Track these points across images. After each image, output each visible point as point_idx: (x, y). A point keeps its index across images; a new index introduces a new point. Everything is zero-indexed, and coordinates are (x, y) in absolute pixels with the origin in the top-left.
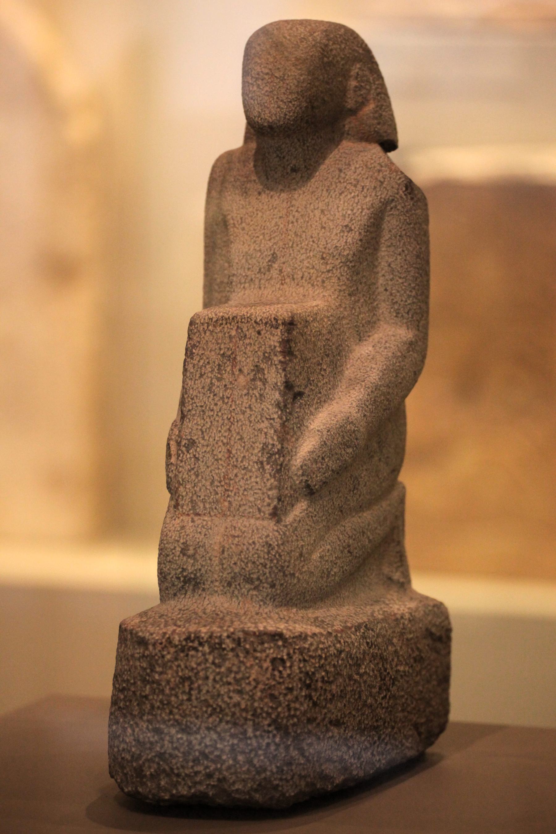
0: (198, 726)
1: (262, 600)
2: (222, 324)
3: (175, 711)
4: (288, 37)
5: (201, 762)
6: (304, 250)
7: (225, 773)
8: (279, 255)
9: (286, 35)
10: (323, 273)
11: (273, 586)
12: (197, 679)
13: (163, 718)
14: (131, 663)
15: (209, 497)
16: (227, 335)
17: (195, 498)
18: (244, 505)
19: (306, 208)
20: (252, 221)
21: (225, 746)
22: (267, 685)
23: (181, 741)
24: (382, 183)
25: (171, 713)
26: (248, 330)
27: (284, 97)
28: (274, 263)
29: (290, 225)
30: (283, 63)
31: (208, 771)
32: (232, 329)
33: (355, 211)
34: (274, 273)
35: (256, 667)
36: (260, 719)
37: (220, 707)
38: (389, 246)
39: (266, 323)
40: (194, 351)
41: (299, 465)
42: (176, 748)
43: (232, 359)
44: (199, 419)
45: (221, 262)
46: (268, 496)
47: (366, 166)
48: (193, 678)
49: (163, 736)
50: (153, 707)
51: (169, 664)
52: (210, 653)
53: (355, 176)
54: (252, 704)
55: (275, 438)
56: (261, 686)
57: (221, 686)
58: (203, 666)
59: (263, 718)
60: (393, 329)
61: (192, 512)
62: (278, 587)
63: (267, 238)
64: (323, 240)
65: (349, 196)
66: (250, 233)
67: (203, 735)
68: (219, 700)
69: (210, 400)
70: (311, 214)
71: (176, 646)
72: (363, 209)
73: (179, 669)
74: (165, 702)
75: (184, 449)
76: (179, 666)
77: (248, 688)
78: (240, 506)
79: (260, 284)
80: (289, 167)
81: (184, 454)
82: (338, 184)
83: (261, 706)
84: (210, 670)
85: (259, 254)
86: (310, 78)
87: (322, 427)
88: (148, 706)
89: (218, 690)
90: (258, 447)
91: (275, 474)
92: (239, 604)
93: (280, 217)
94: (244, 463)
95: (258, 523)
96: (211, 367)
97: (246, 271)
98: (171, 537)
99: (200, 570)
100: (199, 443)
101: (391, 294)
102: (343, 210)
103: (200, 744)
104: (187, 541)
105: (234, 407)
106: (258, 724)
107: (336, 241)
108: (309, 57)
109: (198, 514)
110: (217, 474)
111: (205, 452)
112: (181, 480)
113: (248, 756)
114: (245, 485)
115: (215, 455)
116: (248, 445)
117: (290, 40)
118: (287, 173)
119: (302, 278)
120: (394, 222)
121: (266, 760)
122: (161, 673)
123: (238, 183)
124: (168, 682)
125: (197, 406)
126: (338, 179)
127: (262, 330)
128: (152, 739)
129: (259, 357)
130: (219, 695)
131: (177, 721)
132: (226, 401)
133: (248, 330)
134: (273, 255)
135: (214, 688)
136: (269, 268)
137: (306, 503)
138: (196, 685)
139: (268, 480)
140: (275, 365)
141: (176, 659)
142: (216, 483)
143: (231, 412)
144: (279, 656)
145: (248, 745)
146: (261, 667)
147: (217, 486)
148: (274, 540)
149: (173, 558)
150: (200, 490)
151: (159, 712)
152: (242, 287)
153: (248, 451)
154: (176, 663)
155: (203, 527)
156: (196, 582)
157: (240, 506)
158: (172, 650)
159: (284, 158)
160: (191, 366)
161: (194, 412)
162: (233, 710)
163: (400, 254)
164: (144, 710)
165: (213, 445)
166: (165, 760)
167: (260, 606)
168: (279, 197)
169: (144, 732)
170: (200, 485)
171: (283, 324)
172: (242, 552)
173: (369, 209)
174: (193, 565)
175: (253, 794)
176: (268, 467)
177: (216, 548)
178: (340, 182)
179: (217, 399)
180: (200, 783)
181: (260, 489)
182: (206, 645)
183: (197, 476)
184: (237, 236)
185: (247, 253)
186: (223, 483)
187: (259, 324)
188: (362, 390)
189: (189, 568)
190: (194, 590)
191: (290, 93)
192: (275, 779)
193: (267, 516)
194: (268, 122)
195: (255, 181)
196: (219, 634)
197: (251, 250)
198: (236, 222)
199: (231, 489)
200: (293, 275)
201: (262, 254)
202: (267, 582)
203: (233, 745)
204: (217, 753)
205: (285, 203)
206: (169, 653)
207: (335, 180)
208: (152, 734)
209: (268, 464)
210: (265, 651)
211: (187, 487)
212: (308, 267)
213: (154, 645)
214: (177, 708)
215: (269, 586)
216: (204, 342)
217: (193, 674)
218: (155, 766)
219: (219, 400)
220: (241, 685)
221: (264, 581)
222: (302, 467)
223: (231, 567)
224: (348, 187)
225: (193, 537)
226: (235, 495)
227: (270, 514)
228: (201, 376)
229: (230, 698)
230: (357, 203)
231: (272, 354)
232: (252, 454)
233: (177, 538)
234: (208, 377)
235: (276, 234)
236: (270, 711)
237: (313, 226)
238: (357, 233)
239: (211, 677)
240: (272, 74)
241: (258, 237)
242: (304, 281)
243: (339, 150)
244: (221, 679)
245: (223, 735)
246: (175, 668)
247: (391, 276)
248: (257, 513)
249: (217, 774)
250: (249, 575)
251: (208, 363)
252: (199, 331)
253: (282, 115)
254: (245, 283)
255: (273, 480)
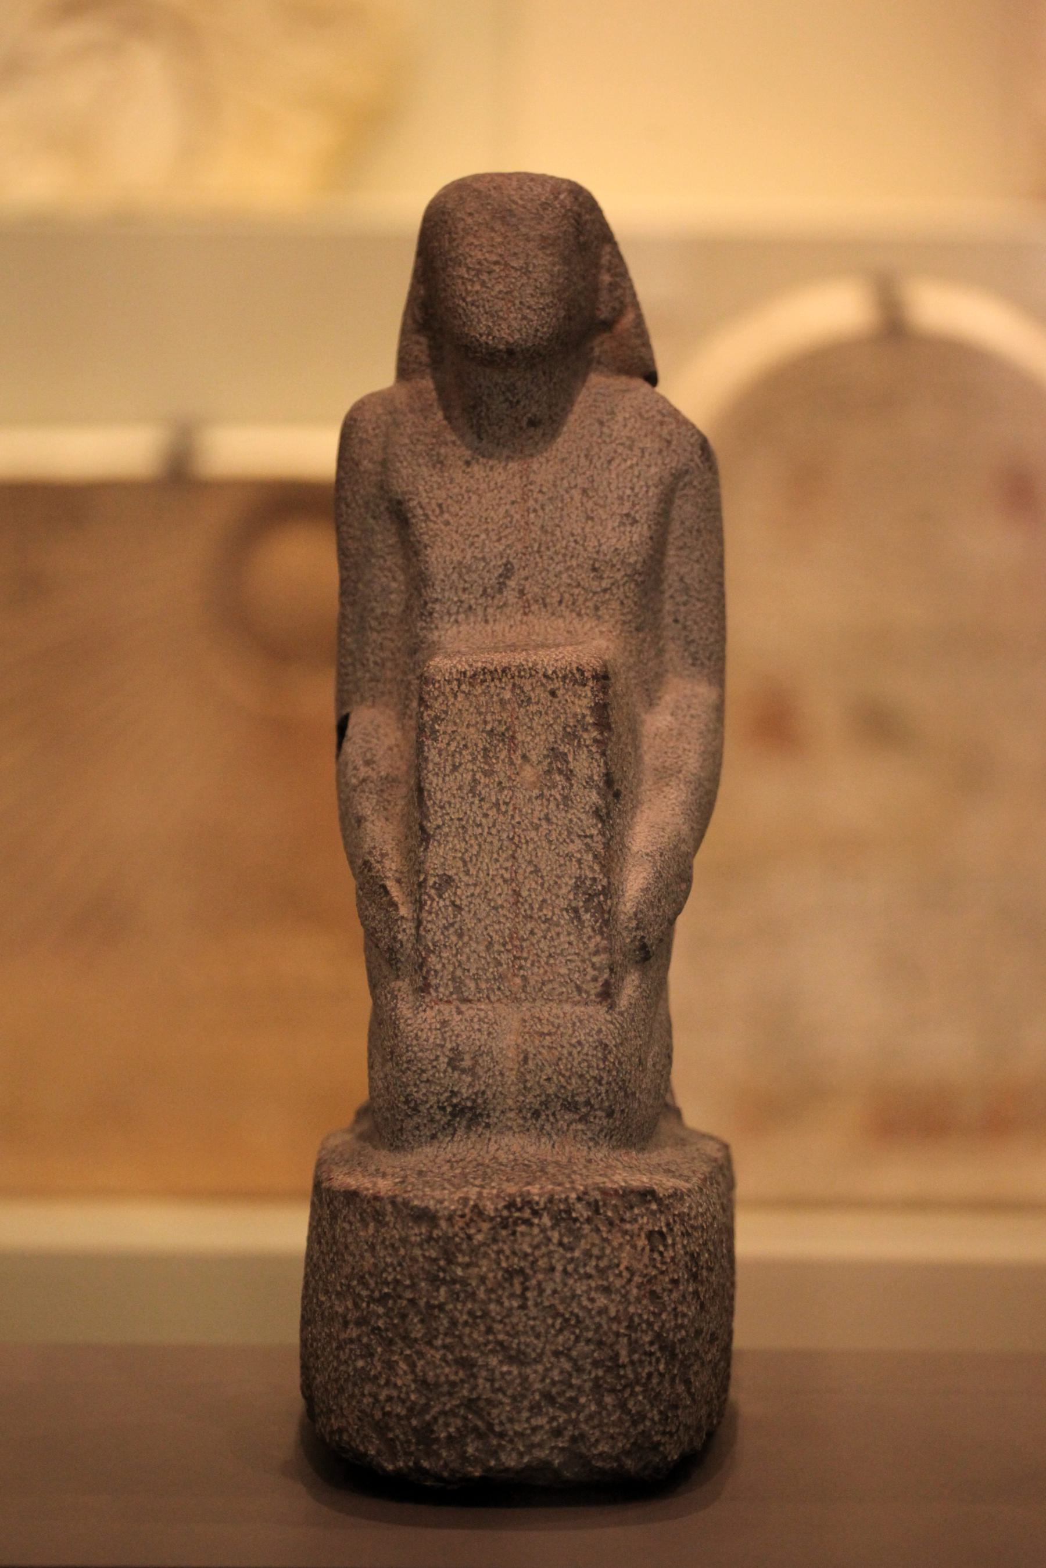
0: (538, 1351)
1: (591, 1139)
2: (483, 681)
3: (498, 1327)
4: (521, 202)
5: (544, 1410)
6: (560, 557)
7: (583, 1426)
8: (516, 567)
9: (516, 198)
10: (595, 593)
11: (610, 1114)
12: (535, 1272)
13: (475, 1340)
14: (402, 1252)
15: (485, 971)
16: (495, 699)
17: (459, 973)
18: (550, 981)
19: (555, 485)
20: (461, 509)
21: (585, 1381)
22: (645, 1276)
23: (508, 1378)
24: (669, 442)
25: (489, 1330)
26: (533, 689)
27: (532, 302)
28: (509, 578)
29: (532, 515)
30: (521, 244)
31: (555, 1424)
32: (503, 688)
33: (637, 490)
34: (510, 595)
35: (628, 1247)
36: (639, 1334)
37: (577, 1316)
38: (681, 548)
39: (565, 677)
40: (437, 727)
41: (631, 912)
42: (500, 1390)
43: (508, 738)
44: (456, 841)
45: (384, 579)
46: (593, 965)
47: (640, 415)
48: (528, 1271)
49: (475, 1370)
50: (454, 1323)
51: (482, 1249)
52: (553, 1228)
53: (625, 432)
54: (626, 1309)
55: (597, 867)
56: (637, 1279)
57: (576, 1281)
58: (544, 1250)
59: (642, 1331)
60: (689, 686)
61: (454, 996)
62: (617, 1115)
63: (495, 538)
64: (593, 539)
65: (623, 466)
66: (461, 530)
67: (549, 1365)
68: (574, 1305)
69: (475, 808)
70: (566, 496)
71: (492, 1219)
72: (648, 487)
73: (502, 1257)
74: (479, 1313)
75: (433, 892)
76: (500, 1252)
77: (618, 1283)
78: (543, 984)
79: (485, 616)
80: (525, 418)
81: (433, 900)
82: (603, 446)
83: (639, 1311)
84: (556, 1256)
85: (483, 564)
86: (567, 269)
87: (651, 848)
88: (445, 1322)
89: (571, 1288)
90: (566, 884)
91: (601, 927)
92: (553, 1146)
93: (513, 503)
94: (545, 911)
95: (579, 1010)
96: (472, 754)
97: (460, 593)
98: (427, 1040)
99: (483, 1093)
100: (460, 881)
101: (685, 628)
102: (618, 488)
103: (543, 1380)
104: (458, 1045)
105: (518, 819)
106: (636, 1341)
107: (614, 540)
108: (560, 235)
109: (467, 1001)
110: (497, 932)
111: (472, 895)
112: (430, 944)
113: (620, 1395)
114: (549, 947)
115: (489, 900)
116: (549, 881)
117: (524, 207)
118: (521, 428)
119: (560, 602)
120: (689, 508)
121: (645, 1401)
122: (466, 1266)
123: (420, 447)
124: (483, 1279)
125: (451, 819)
126: (600, 437)
127: (559, 689)
128: (452, 1378)
129: (556, 734)
130: (574, 1296)
131: (501, 1343)
132: (503, 808)
133: (533, 689)
134: (505, 565)
135: (565, 1285)
136: (501, 587)
137: (636, 975)
138: (534, 1282)
139: (590, 938)
140: (587, 747)
141: (495, 1240)
142: (496, 947)
143: (514, 827)
144: (657, 1229)
145: (619, 1377)
146: (634, 1247)
147: (499, 953)
148: (610, 1037)
149: (433, 1075)
150: (469, 959)
151: (467, 1330)
152: (452, 619)
153: (549, 890)
154: (495, 1248)
155: (480, 1020)
156: (474, 1114)
157: (543, 984)
158: (486, 1226)
159: (518, 402)
160: (434, 752)
161: (447, 830)
162: (597, 1319)
163: (698, 561)
164: (437, 1329)
165: (487, 884)
166: (478, 1413)
167: (589, 1148)
168: (505, 468)
169: (436, 1367)
170: (467, 950)
171: (593, 677)
172: (560, 1059)
173: (656, 487)
174: (471, 1085)
175: (623, 1458)
176: (588, 916)
177: (510, 1055)
178: (604, 442)
179: (486, 806)
180: (540, 1445)
181: (578, 954)
182: (545, 1214)
183: (460, 936)
184: (437, 535)
185: (460, 563)
186: (509, 947)
187: (552, 680)
188: (682, 786)
189: (464, 1091)
190: (468, 1128)
191: (542, 294)
192: (657, 1433)
193: (593, 997)
194: (507, 342)
195: (454, 443)
196: (563, 1196)
197: (468, 557)
198: (430, 513)
199: (525, 955)
200: (543, 599)
201: (488, 564)
202: (601, 1109)
203: (597, 1378)
204: (571, 1394)
205: (517, 479)
206: (479, 1231)
207: (595, 438)
208: (454, 1368)
209: (587, 911)
210: (636, 1220)
211: (444, 955)
212: (569, 585)
213: (450, 1219)
214: (501, 1322)
215: (603, 1114)
216: (455, 711)
217: (527, 1264)
218: (459, 1422)
219: (491, 808)
220: (607, 1280)
221: (596, 1106)
222: (635, 914)
223: (541, 1086)
224: (619, 451)
225: (468, 1038)
226: (533, 965)
227: (598, 995)
228: (455, 768)
229: (592, 1300)
230: (638, 477)
231: (579, 727)
232: (558, 896)
233: (438, 1042)
234: (468, 771)
235: (509, 531)
236: (652, 1319)
237: (573, 516)
238: (646, 527)
239: (559, 1268)
240: (506, 265)
241: (477, 536)
242: (563, 607)
243: (588, 389)
244: (576, 1270)
245: (580, 1363)
246: (493, 1256)
247: (685, 598)
248: (575, 993)
249: (570, 1428)
250: (573, 1096)
251: (465, 746)
252: (443, 694)
253: (531, 332)
254: (458, 613)
255: (598, 938)
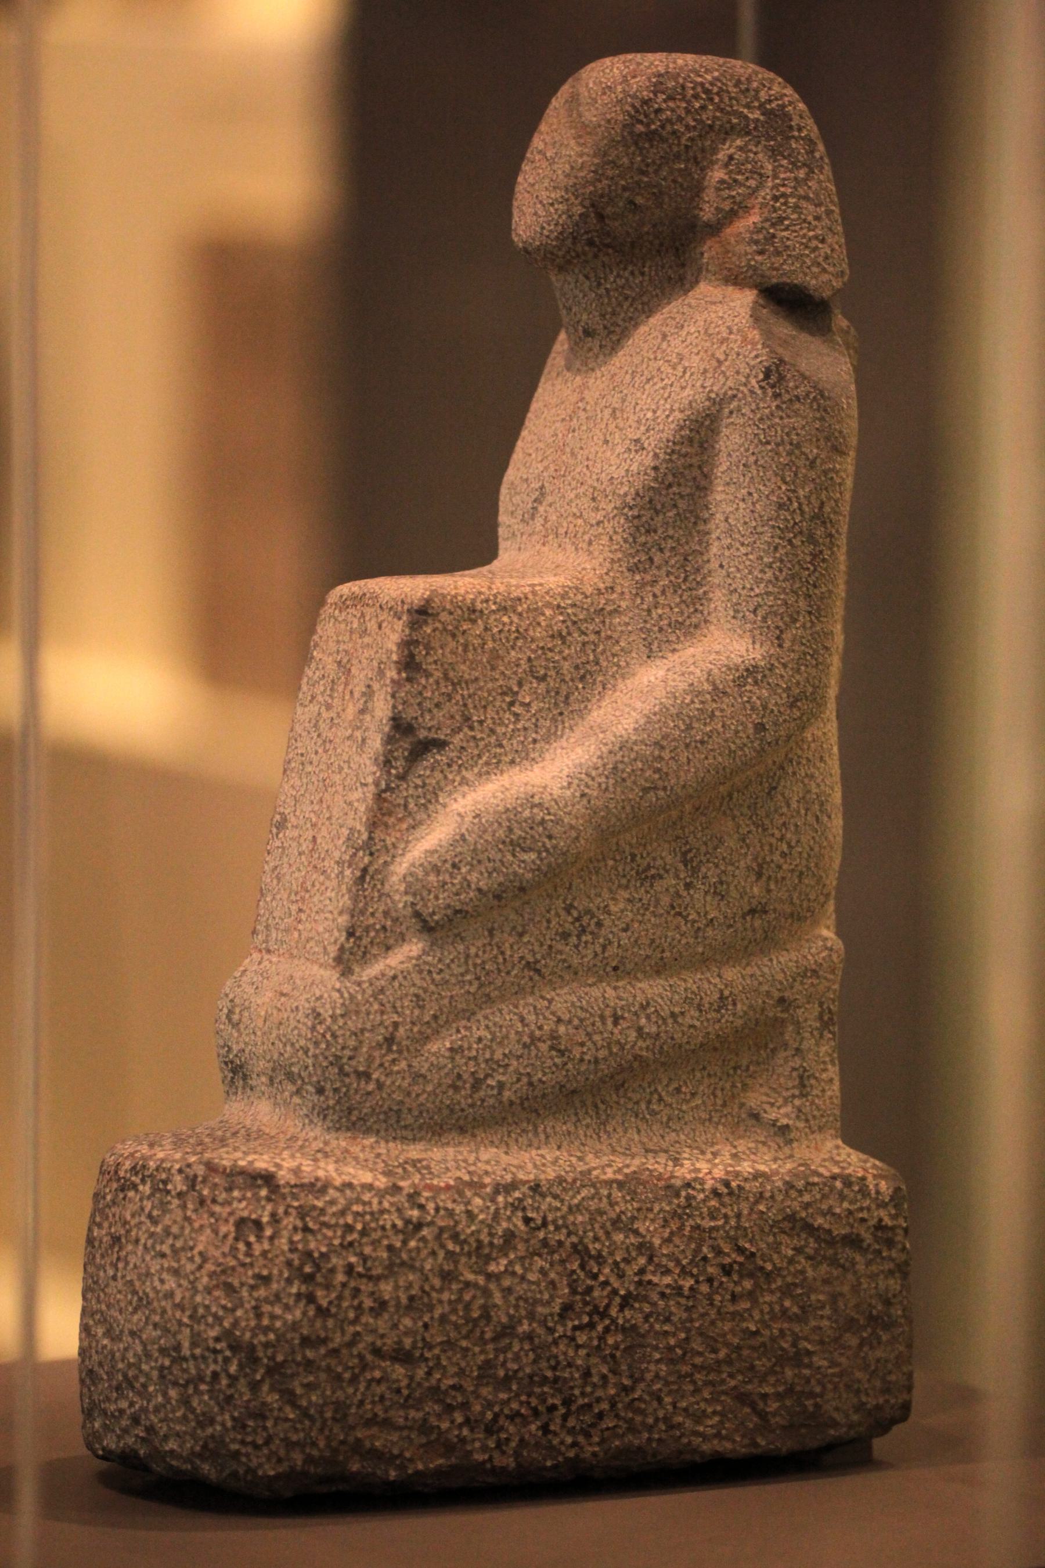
1: (307, 1116)
11: (320, 1091)
22: (219, 1265)
35: (208, 1231)
36: (202, 1327)
38: (728, 484)
54: (192, 1297)
56: (210, 1267)
59: (207, 1324)
62: (329, 1093)
77: (190, 1267)
83: (207, 1302)
86: (596, 161)
120: (736, 438)
121: (212, 1403)
130: (148, 1274)
137: (420, 945)
144: (254, 1216)
146: (216, 1232)
148: (328, 1006)
192: (233, 1441)
202: (310, 1083)
210: (230, 1203)
220: (178, 1261)
229: (162, 1281)
236: (221, 1313)
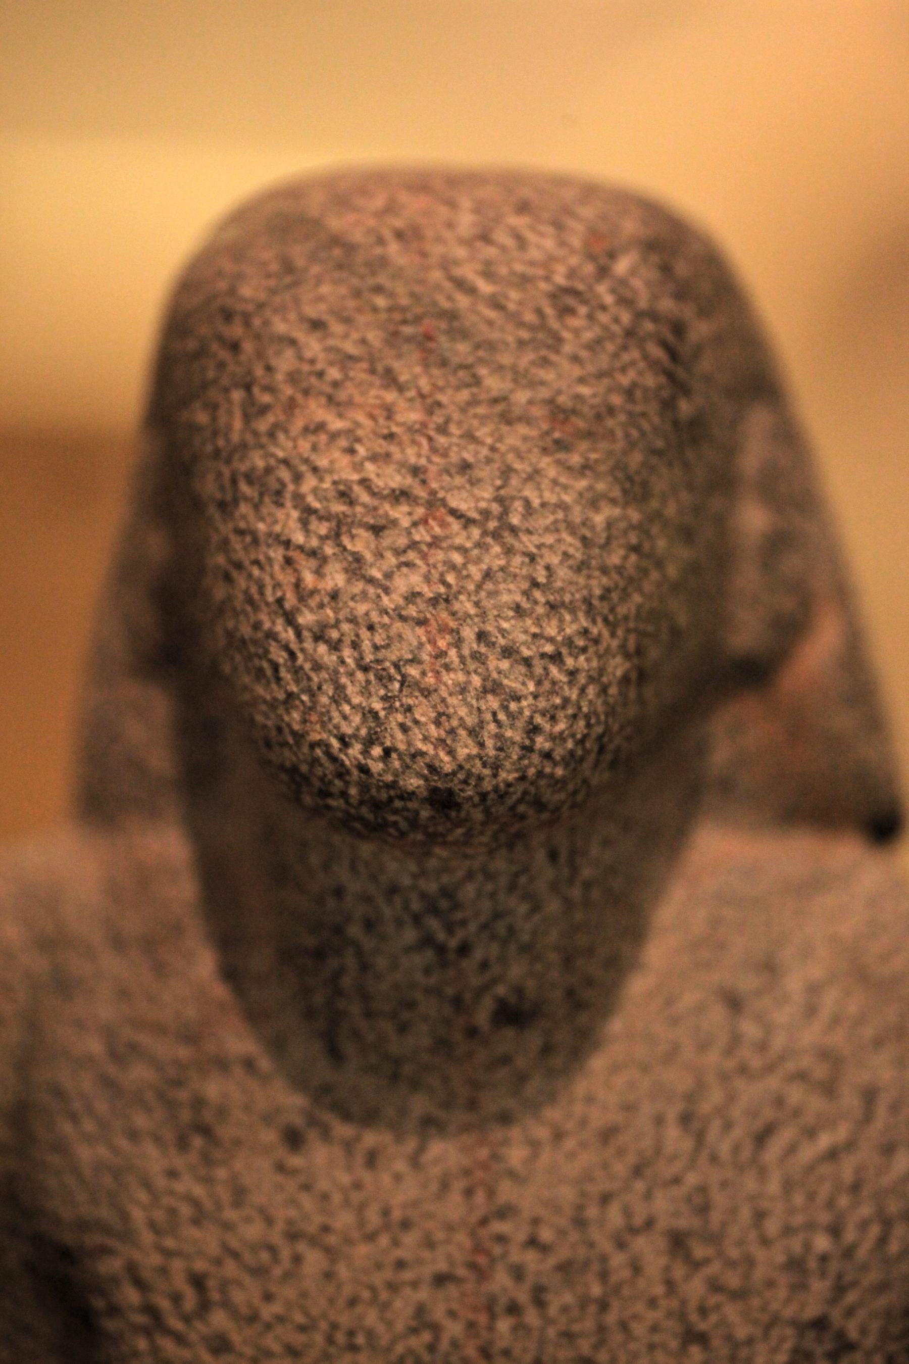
4: (485, 287)
9: (468, 272)
20: (268, 1297)
27: (518, 632)
29: (504, 1325)
30: (483, 433)
33: (850, 1235)
53: (811, 1035)
65: (807, 1153)
70: (618, 1260)
82: (739, 1084)
86: (635, 516)
93: (441, 1280)
108: (617, 400)
118: (472, 1032)
123: (139, 1074)
126: (729, 1051)
159: (464, 949)
168: (415, 1162)
195: (249, 1064)
198: (164, 1304)
205: (455, 1197)
237: (639, 1329)
240: (434, 502)
